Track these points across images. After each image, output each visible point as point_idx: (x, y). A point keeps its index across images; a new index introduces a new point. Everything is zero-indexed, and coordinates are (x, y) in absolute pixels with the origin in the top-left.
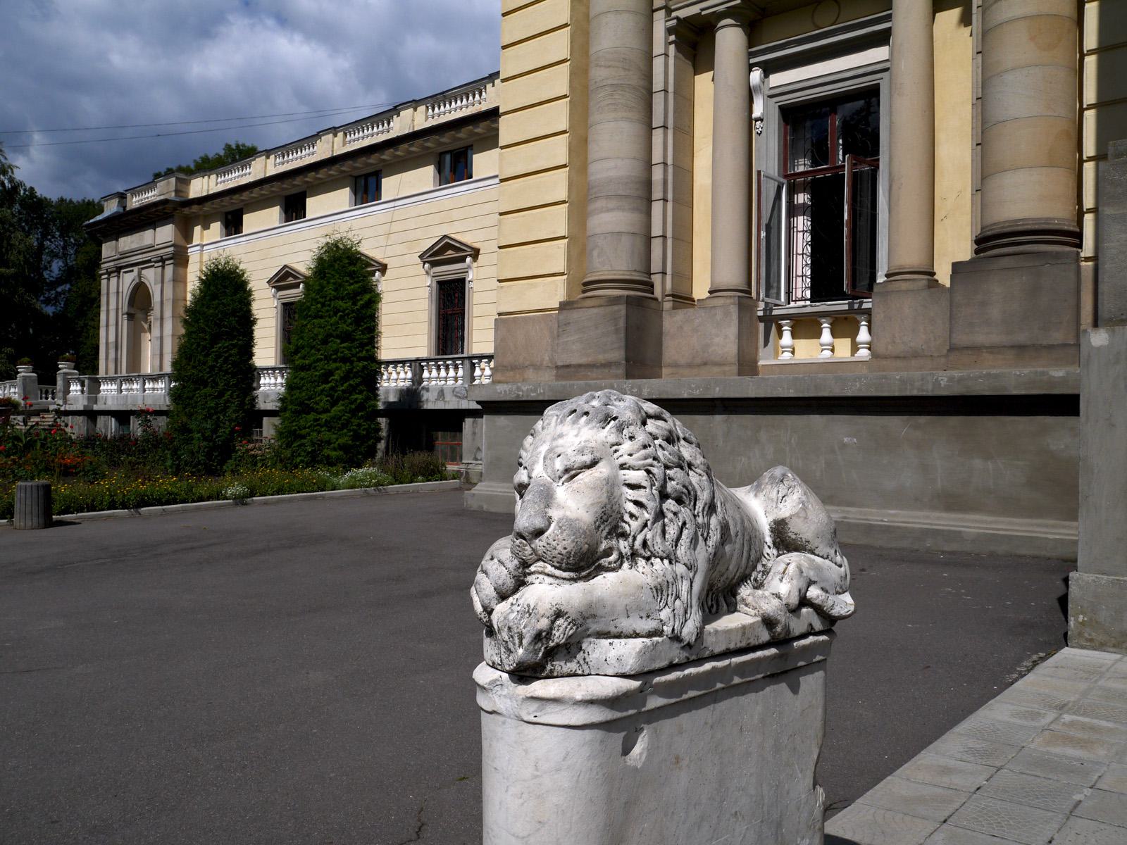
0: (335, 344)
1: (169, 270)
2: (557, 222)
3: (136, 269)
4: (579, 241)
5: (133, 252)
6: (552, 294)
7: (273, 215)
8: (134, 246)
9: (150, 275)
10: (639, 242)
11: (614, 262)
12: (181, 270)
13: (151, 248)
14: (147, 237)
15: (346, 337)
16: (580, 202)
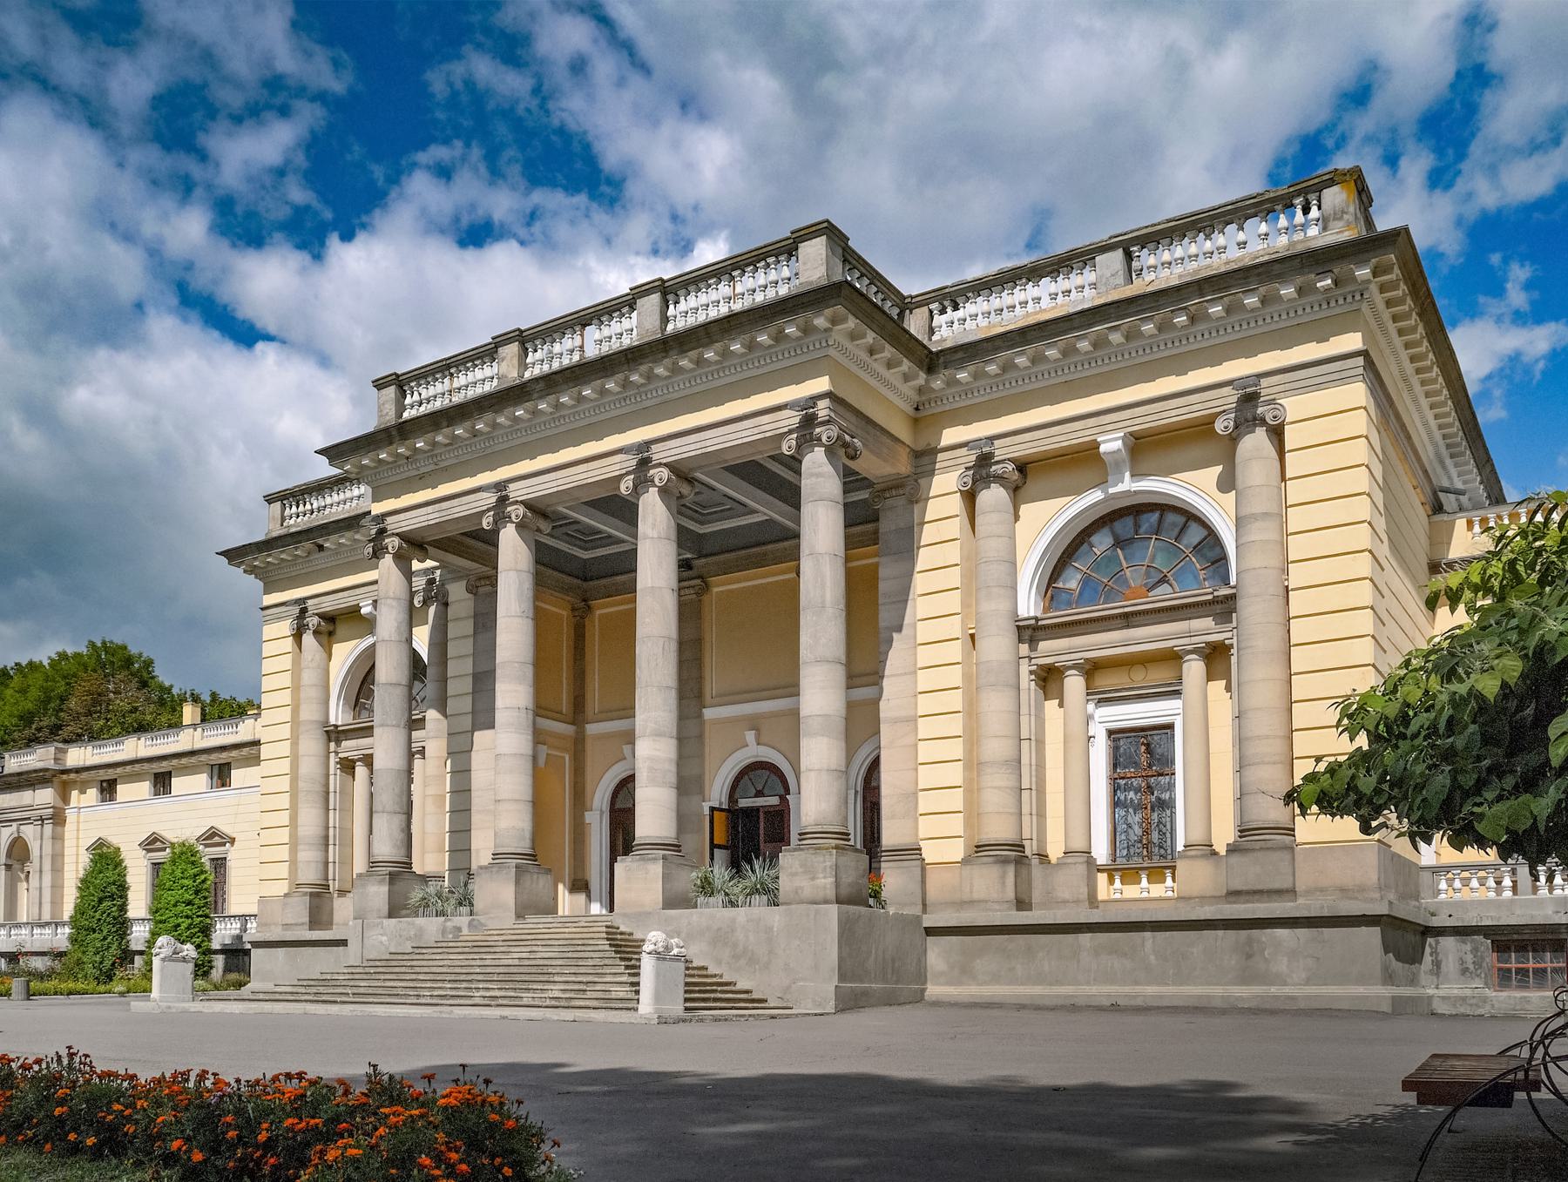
0: (181, 907)
1: (48, 828)
2: (284, 853)
3: (15, 825)
4: (293, 862)
5: (12, 809)
6: (282, 888)
7: (144, 788)
8: (13, 804)
9: (29, 832)
10: (321, 866)
11: (310, 875)
12: (59, 829)
13: (30, 808)
14: (26, 797)
15: (189, 903)
16: (294, 844)
